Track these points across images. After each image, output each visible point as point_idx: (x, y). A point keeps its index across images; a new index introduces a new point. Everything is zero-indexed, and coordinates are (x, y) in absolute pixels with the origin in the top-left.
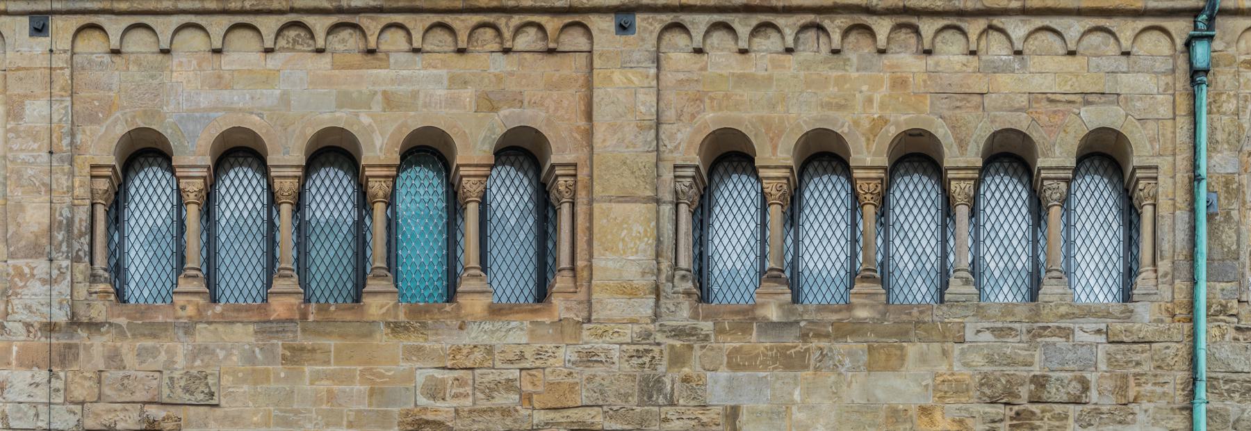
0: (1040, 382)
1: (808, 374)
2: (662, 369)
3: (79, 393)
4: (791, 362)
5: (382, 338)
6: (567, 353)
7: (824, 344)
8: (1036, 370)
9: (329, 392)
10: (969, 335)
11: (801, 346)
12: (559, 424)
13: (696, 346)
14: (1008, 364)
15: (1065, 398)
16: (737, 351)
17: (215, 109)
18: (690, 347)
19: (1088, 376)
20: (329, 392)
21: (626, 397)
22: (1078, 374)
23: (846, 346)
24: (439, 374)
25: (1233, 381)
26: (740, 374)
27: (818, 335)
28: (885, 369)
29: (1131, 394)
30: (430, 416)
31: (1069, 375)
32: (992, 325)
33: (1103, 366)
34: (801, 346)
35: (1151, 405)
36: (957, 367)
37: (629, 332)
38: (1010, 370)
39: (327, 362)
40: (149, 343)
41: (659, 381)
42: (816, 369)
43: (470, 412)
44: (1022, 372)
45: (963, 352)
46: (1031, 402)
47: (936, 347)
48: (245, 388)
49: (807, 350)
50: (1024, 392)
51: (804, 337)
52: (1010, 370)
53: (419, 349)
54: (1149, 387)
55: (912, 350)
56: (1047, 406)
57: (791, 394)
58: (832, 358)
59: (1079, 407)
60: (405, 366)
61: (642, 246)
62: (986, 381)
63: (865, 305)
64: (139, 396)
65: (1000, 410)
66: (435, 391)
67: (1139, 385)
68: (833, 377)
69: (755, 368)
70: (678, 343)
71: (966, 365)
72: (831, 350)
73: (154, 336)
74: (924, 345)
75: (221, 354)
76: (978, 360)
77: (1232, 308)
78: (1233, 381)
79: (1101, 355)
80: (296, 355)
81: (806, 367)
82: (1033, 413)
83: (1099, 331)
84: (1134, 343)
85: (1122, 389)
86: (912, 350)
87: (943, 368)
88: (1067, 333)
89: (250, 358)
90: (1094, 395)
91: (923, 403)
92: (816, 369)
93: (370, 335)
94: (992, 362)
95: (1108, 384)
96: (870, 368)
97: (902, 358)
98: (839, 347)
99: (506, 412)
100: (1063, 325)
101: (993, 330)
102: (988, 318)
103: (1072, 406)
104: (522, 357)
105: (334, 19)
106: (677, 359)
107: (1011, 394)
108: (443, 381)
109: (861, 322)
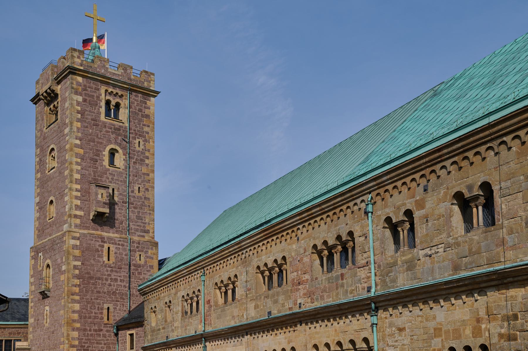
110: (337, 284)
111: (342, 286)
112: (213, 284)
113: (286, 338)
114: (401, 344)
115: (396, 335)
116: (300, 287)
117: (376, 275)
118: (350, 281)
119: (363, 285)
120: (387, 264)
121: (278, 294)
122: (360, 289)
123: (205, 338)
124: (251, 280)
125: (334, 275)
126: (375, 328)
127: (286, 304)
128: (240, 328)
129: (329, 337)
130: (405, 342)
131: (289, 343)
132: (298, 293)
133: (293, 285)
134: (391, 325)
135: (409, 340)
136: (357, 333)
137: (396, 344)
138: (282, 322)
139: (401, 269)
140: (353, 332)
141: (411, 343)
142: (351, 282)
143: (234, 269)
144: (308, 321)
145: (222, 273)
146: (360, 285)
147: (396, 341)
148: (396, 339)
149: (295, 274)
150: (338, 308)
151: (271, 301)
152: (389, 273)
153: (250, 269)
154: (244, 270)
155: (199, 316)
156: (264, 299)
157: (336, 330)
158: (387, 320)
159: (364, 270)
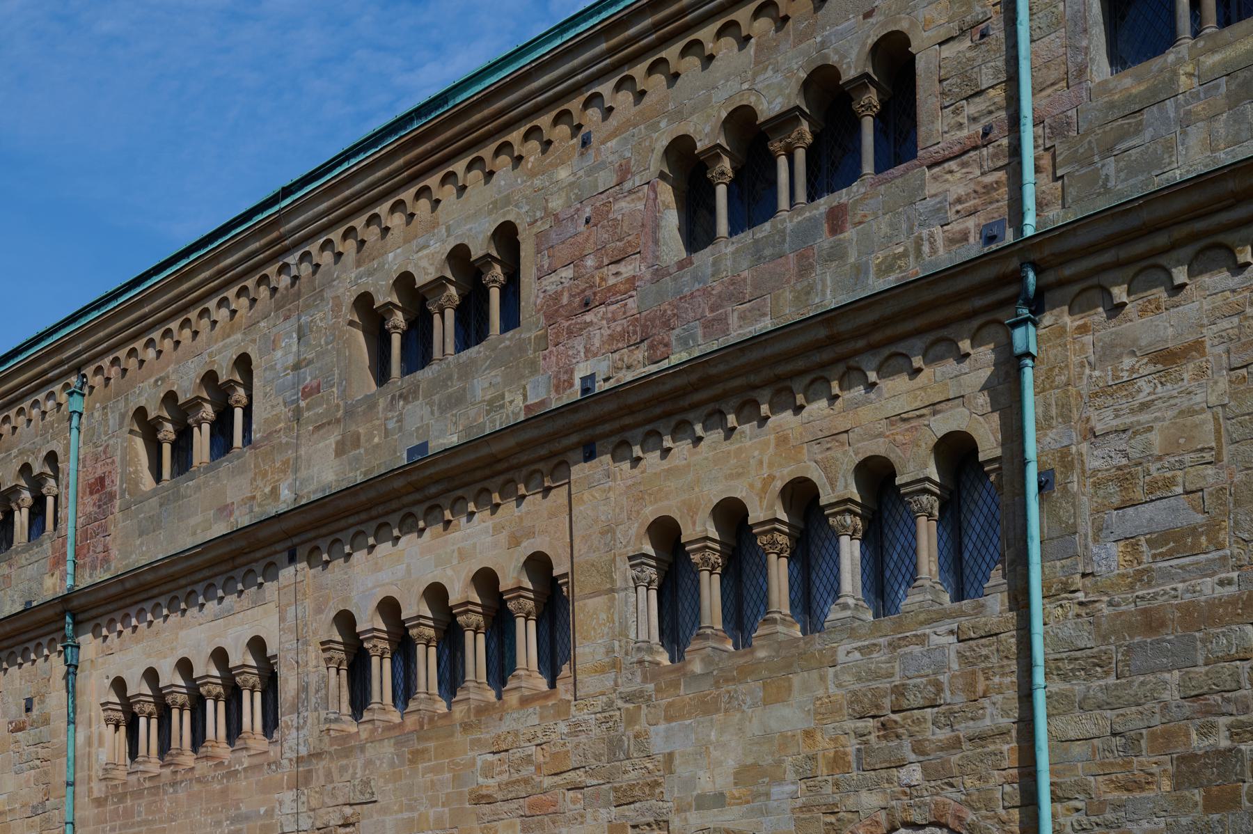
0: (900, 691)
1: (720, 716)
2: (622, 729)
3: (314, 804)
4: (707, 707)
5: (459, 737)
6: (563, 727)
7: (732, 687)
8: (897, 681)
9: (432, 781)
10: (841, 657)
11: (716, 692)
12: (559, 785)
13: (644, 706)
14: (874, 679)
15: (922, 703)
16: (670, 705)
17: (375, 587)
18: (640, 707)
19: (941, 678)
20: (432, 781)
21: (597, 757)
22: (932, 677)
23: (746, 686)
24: (490, 757)
25: (1076, 659)
26: (673, 724)
27: (727, 680)
28: (777, 701)
29: (980, 688)
30: (484, 792)
31: (924, 680)
32: (860, 644)
33: (955, 666)
34: (716, 692)
35: (1000, 697)
36: (832, 689)
37: (601, 702)
38: (874, 685)
39: (430, 760)
40: (344, 762)
41: (621, 740)
42: (726, 711)
43: (507, 784)
44: (884, 685)
45: (836, 676)
46: (894, 712)
47: (815, 674)
48: (390, 786)
49: (719, 695)
50: (887, 703)
51: (717, 684)
52: (874, 685)
53: (479, 740)
54: (997, 679)
55: (796, 680)
56: (908, 713)
57: (709, 736)
58: (737, 699)
59: (936, 710)
60: (471, 754)
61: (606, 630)
62: (855, 698)
63: (763, 646)
64: (341, 801)
65: (871, 723)
66: (488, 771)
67: (987, 679)
68: (739, 715)
69: (683, 717)
70: (631, 706)
71: (839, 686)
72: (736, 691)
73: (347, 757)
74: (806, 674)
75: (378, 763)
76: (847, 678)
77: (1073, 583)
78: (1076, 659)
79: (953, 655)
80: (417, 756)
81: (718, 710)
82: (896, 722)
83: (952, 632)
84: (982, 637)
85: (971, 686)
86: (796, 680)
87: (820, 693)
88: (922, 640)
89: (392, 765)
90: (947, 695)
91: (805, 726)
92: (726, 711)
93: (452, 735)
94: (860, 679)
95: (960, 683)
96: (766, 702)
97: (789, 689)
98: (742, 688)
99: (526, 781)
100: (919, 632)
101: (859, 649)
102: (860, 639)
103: (929, 710)
104: (535, 736)
105: (427, 505)
106: (632, 719)
107: (878, 707)
108: (492, 763)
109: (760, 661)
110: (801, 257)
111: (836, 254)
112: (123, 416)
113: (497, 529)
114: (1170, 414)
115: (1141, 383)
116: (588, 317)
117: (1038, 170)
118: (882, 226)
119: (956, 227)
120: (1112, 106)
121: (467, 371)
122: (940, 243)
123: (73, 617)
124: (320, 355)
125: (789, 226)
126: (1028, 374)
127: (508, 397)
128: (264, 533)
129: (739, 475)
130: (1198, 399)
131: (515, 542)
132: (579, 344)
133: (551, 318)
134: (1108, 353)
135: (1223, 384)
136: (907, 426)
137: (1144, 417)
138: (495, 460)
139: (1197, 107)
140: (882, 426)
141: (1233, 395)
142: (885, 229)
143: (238, 336)
144: (628, 435)
145: (170, 369)
146: (937, 230)
147: (1144, 406)
148: (1141, 398)
149: (567, 273)
150: (822, 333)
151: (431, 404)
152: (1122, 138)
153: (321, 317)
154: (291, 325)
155: (47, 545)
156: (392, 405)
157: (782, 440)
158: (1088, 339)
159: (964, 165)
